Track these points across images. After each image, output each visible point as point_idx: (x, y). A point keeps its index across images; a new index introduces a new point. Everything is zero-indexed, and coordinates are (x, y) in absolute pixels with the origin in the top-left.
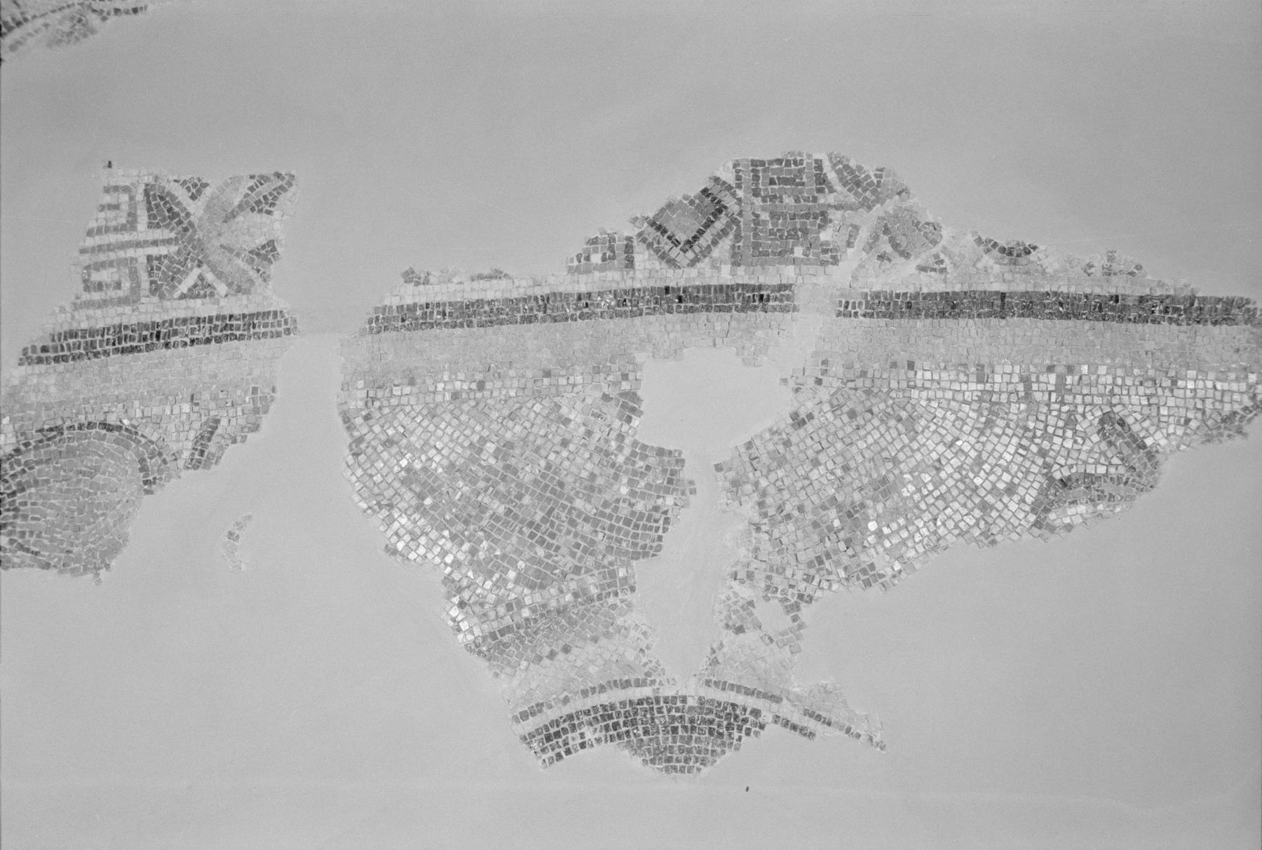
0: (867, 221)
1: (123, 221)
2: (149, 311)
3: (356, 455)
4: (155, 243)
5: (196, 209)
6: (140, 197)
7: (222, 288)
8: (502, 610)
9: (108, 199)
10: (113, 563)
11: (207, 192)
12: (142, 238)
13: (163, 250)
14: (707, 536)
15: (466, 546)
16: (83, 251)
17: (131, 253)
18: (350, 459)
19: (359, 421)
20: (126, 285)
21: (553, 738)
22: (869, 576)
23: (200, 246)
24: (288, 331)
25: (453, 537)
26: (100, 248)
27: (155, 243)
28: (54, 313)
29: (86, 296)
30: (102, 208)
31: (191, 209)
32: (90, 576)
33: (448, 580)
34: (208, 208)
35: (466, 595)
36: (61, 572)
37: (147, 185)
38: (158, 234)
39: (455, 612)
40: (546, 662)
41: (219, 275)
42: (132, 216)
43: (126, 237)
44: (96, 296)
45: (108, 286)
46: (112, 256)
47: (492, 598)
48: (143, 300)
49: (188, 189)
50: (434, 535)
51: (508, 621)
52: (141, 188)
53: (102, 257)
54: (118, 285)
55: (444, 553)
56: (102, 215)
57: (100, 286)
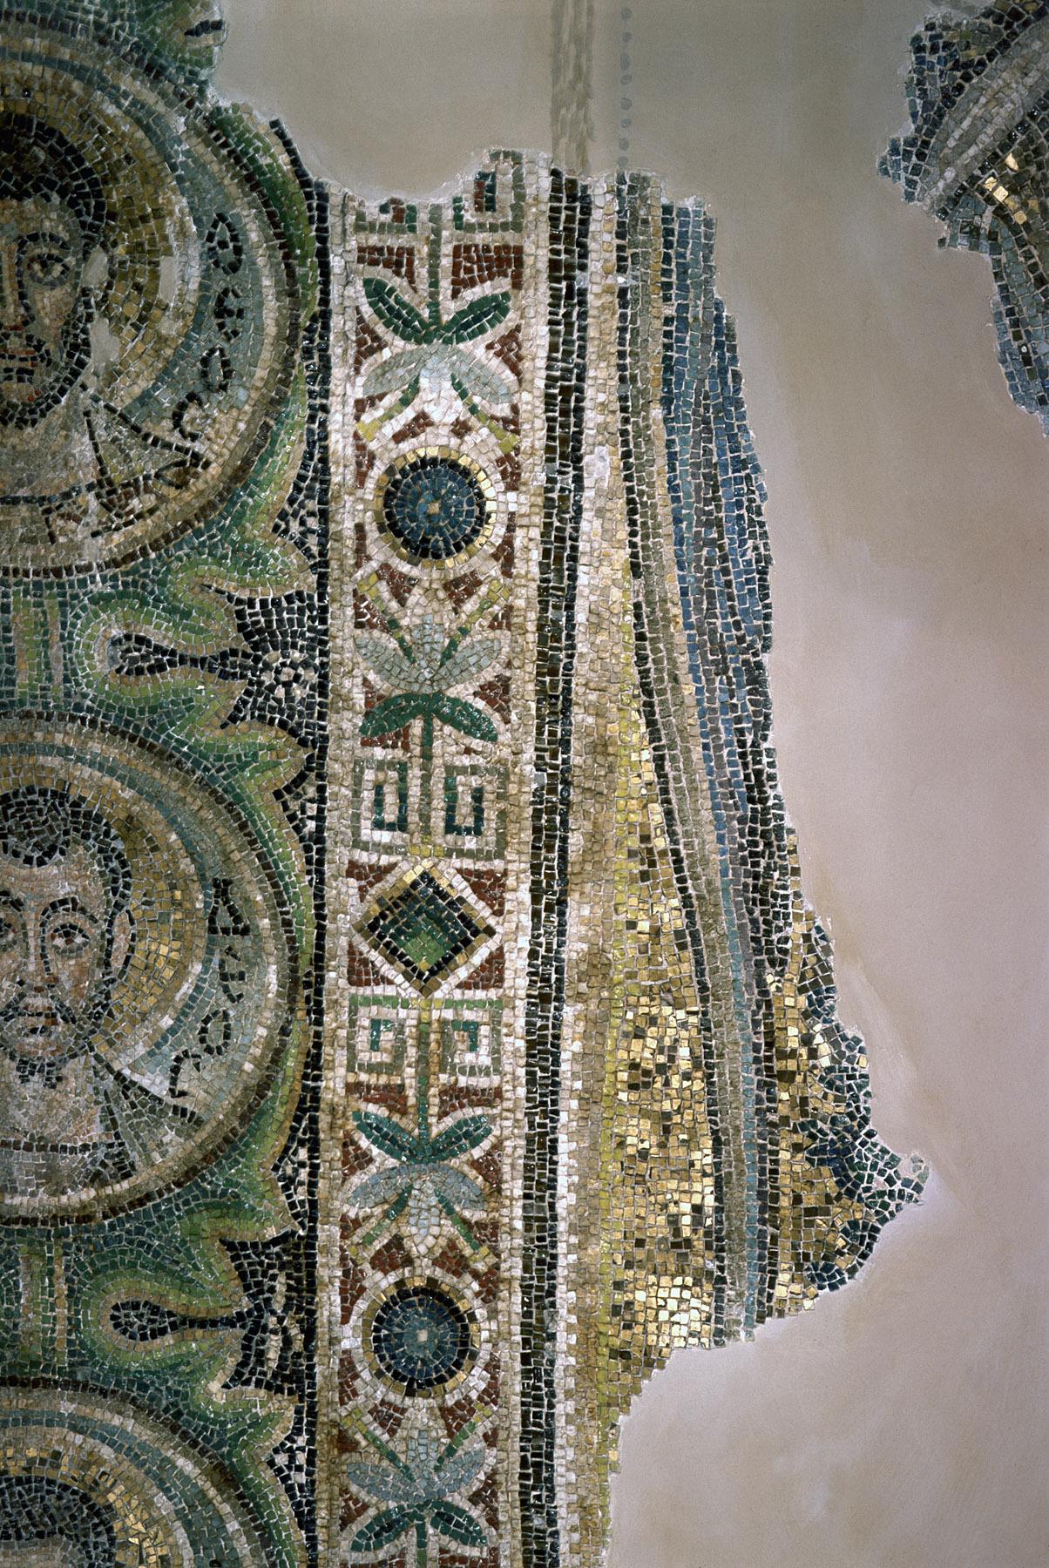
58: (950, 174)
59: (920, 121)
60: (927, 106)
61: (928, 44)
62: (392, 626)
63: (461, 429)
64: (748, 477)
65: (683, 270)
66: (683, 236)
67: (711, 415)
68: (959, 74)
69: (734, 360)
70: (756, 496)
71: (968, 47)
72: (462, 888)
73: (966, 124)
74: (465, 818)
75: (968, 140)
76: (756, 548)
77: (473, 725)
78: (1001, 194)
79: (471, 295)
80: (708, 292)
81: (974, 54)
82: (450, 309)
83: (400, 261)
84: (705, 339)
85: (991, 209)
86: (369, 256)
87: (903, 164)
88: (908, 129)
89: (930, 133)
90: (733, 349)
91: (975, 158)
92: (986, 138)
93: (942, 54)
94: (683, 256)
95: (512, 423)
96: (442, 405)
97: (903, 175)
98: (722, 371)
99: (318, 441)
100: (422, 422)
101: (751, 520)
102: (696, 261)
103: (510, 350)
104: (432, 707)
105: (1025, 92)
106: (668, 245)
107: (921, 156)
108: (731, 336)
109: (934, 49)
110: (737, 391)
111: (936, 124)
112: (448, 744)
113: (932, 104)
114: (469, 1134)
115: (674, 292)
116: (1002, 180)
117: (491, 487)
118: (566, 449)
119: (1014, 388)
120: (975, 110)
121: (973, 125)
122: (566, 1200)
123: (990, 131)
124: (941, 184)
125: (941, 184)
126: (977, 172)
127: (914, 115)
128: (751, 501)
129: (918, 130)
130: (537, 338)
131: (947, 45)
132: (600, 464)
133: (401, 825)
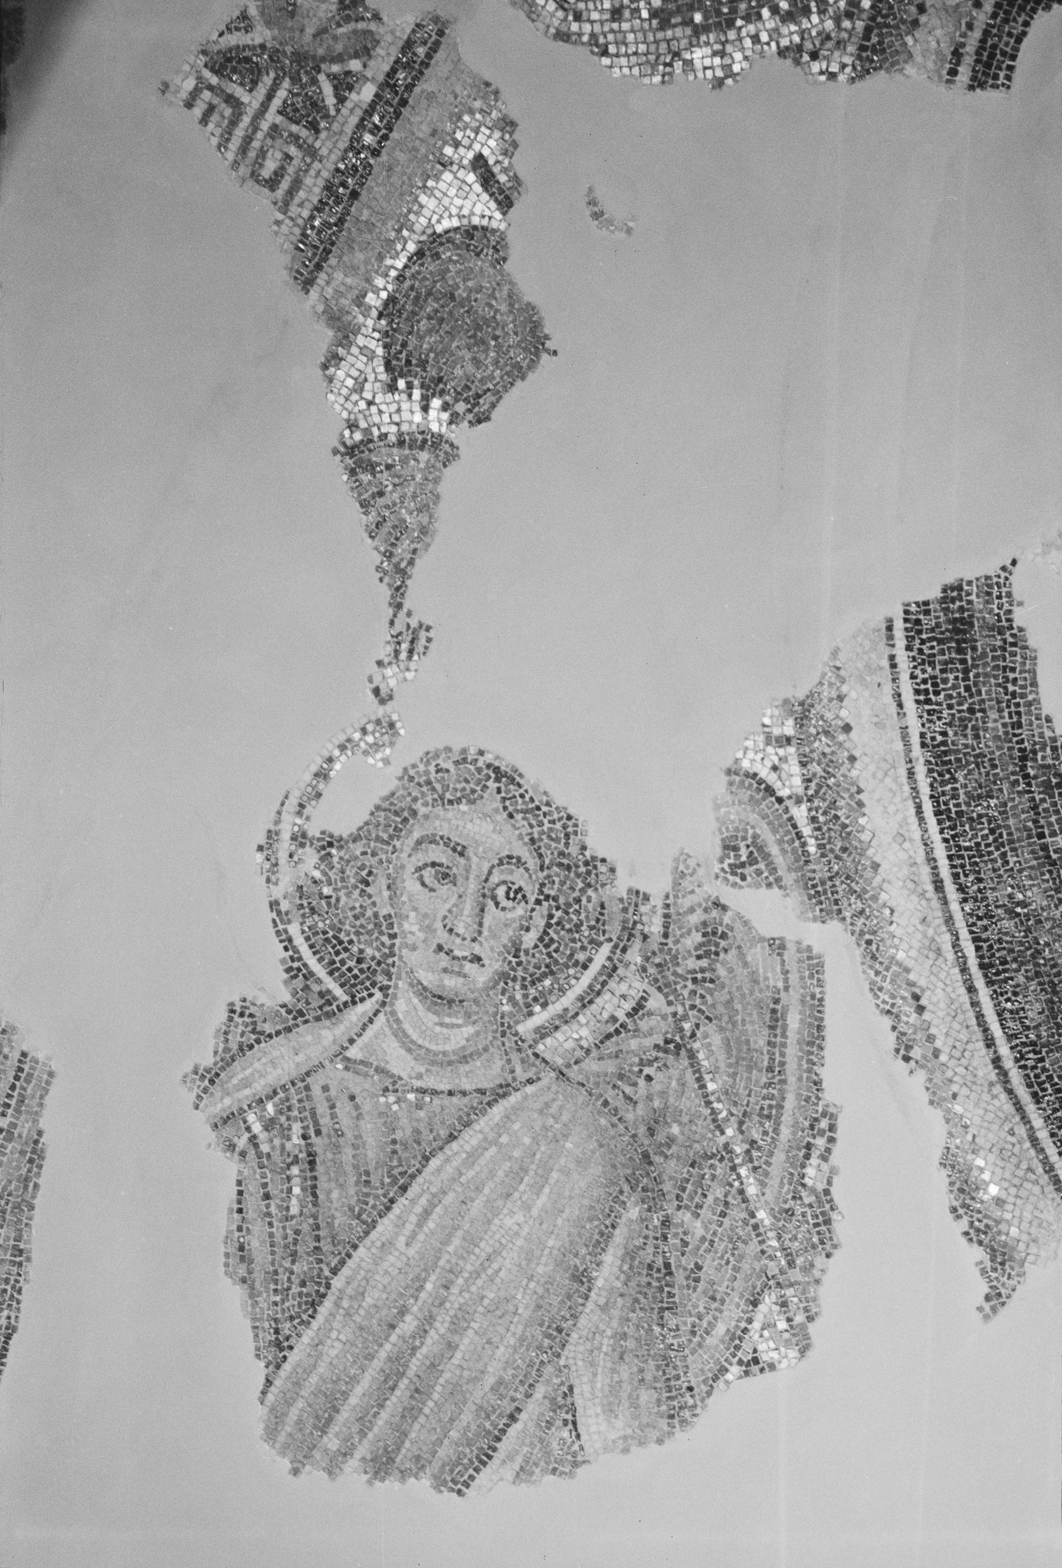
1: (228, 112)
2: (331, 148)
3: (605, 53)
4: (270, 97)
5: (262, 34)
6: (214, 80)
7: (355, 65)
8: (847, 24)
9: (198, 111)
10: (546, 331)
11: (253, 12)
12: (256, 105)
13: (282, 94)
15: (765, 13)
16: (235, 165)
17: (265, 126)
18: (606, 61)
19: (575, 27)
20: (293, 150)
23: (299, 57)
24: (441, 33)
25: (747, 19)
26: (244, 150)
27: (270, 97)
28: (276, 233)
29: (280, 193)
30: (204, 120)
31: (258, 41)
32: (545, 357)
33: (782, 53)
34: (268, 24)
35: (808, 45)
36: (523, 378)
37: (206, 66)
38: (262, 91)
39: (816, 67)
40: (923, 19)
41: (339, 59)
42: (231, 100)
43: (246, 120)
44: (285, 184)
45: (282, 168)
46: (256, 144)
47: (829, 25)
48: (317, 145)
49: (237, 29)
50: (732, 35)
51: (860, 25)
52: (207, 74)
53: (252, 154)
54: (288, 157)
55: (756, 39)
56: (211, 126)
57: (279, 174)
58: (227, 1101)
59: (218, 1058)
60: (227, 1050)
61: (239, 1010)
64: (20, 1264)
65: (21, 1101)
66: (30, 1075)
67: (9, 1208)
68: (254, 1037)
69: (38, 1175)
70: (21, 1279)
71: (265, 1021)
73: (248, 1072)
75: (246, 1083)
76: (9, 1318)
78: (257, 1128)
80: (35, 1121)
81: (268, 1028)
84: (22, 1153)
85: (247, 1135)
87: (198, 1083)
88: (208, 1060)
89: (223, 1069)
90: (40, 1167)
91: (247, 1097)
92: (260, 1087)
93: (246, 1019)
94: (25, 1089)
97: (196, 1090)
98: (27, 1179)
101: (12, 1296)
102: (33, 1097)
105: (293, 1066)
106: (17, 1078)
107: (212, 1082)
108: (42, 1158)
109: (242, 1015)
110: (34, 1197)
111: (228, 1065)
113: (230, 1050)
115: (10, 1111)
116: (260, 1118)
119: (226, 1265)
120: (257, 1065)
121: (252, 1074)
123: (263, 1082)
124: (219, 1106)
125: (219, 1106)
126: (246, 1108)
127: (216, 1053)
128: (17, 1281)
129: (215, 1064)
131: (251, 1015)
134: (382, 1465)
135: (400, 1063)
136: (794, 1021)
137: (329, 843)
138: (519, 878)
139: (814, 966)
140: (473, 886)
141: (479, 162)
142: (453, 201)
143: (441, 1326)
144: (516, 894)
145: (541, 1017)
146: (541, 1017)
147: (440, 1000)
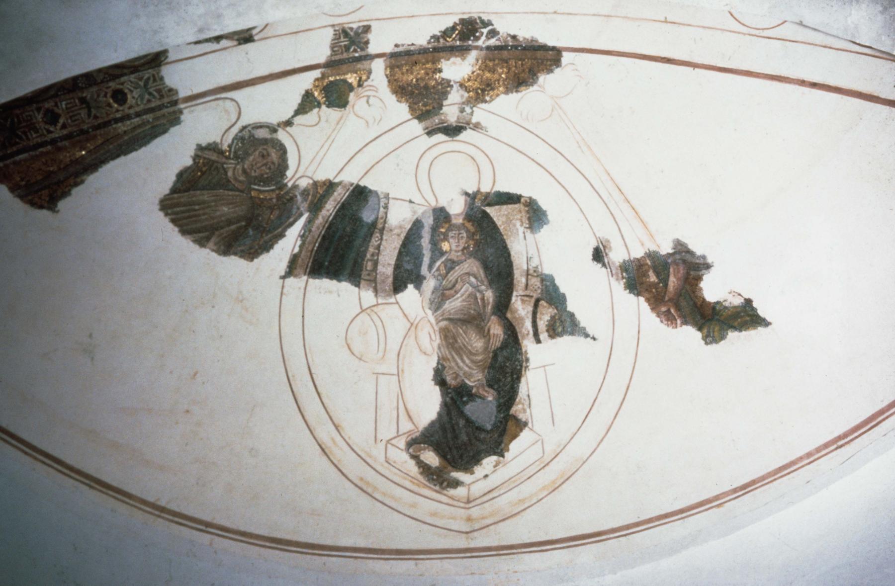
0: (485, 31)
2: (345, 55)
5: (352, 34)
14: (455, 96)
21: (430, 133)
22: (486, 102)
62: (98, 96)
63: (133, 98)
72: (61, 121)
74: (73, 119)
77: (89, 115)
79: (155, 93)
82: (151, 90)
83: (155, 80)
86: (154, 76)
95: (138, 105)
96: (136, 93)
99: (122, 75)
100: (131, 91)
103: (149, 101)
104: (89, 108)
112: (83, 113)
114: (21, 138)
117: (127, 106)
118: (138, 115)
122: (18, 158)
130: (153, 105)
132: (136, 121)
133: (67, 108)
134: (173, 221)
135: (230, 174)
136: (291, 220)
137: (252, 136)
138: (272, 167)
139: (301, 215)
140: (265, 161)
141: (360, 78)
142: (352, 79)
143: (201, 212)
144: (270, 168)
145: (256, 187)
146: (256, 187)
147: (244, 171)
